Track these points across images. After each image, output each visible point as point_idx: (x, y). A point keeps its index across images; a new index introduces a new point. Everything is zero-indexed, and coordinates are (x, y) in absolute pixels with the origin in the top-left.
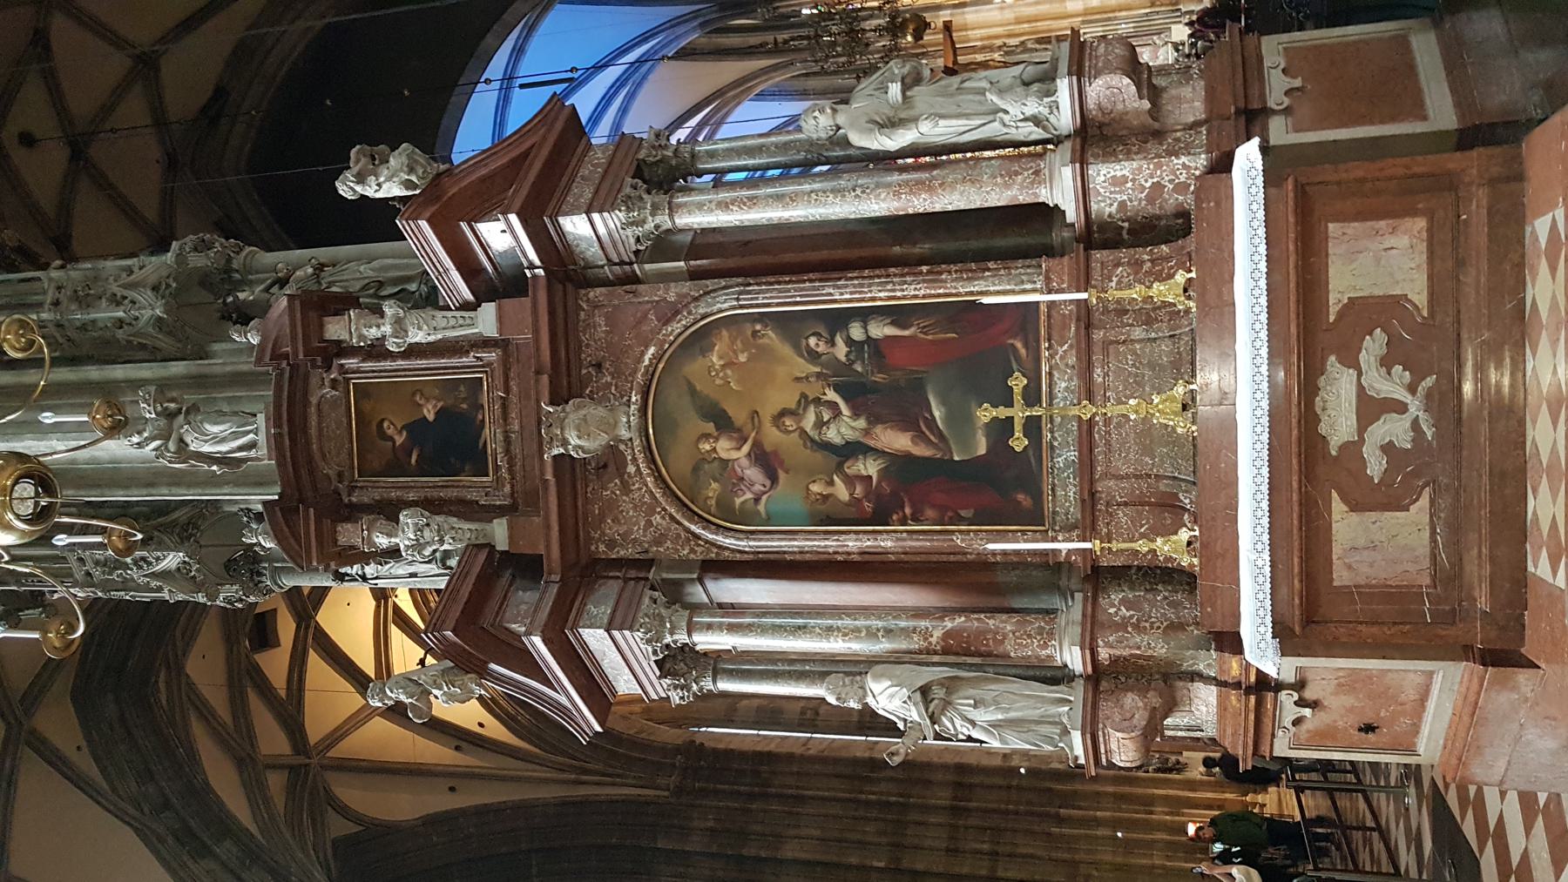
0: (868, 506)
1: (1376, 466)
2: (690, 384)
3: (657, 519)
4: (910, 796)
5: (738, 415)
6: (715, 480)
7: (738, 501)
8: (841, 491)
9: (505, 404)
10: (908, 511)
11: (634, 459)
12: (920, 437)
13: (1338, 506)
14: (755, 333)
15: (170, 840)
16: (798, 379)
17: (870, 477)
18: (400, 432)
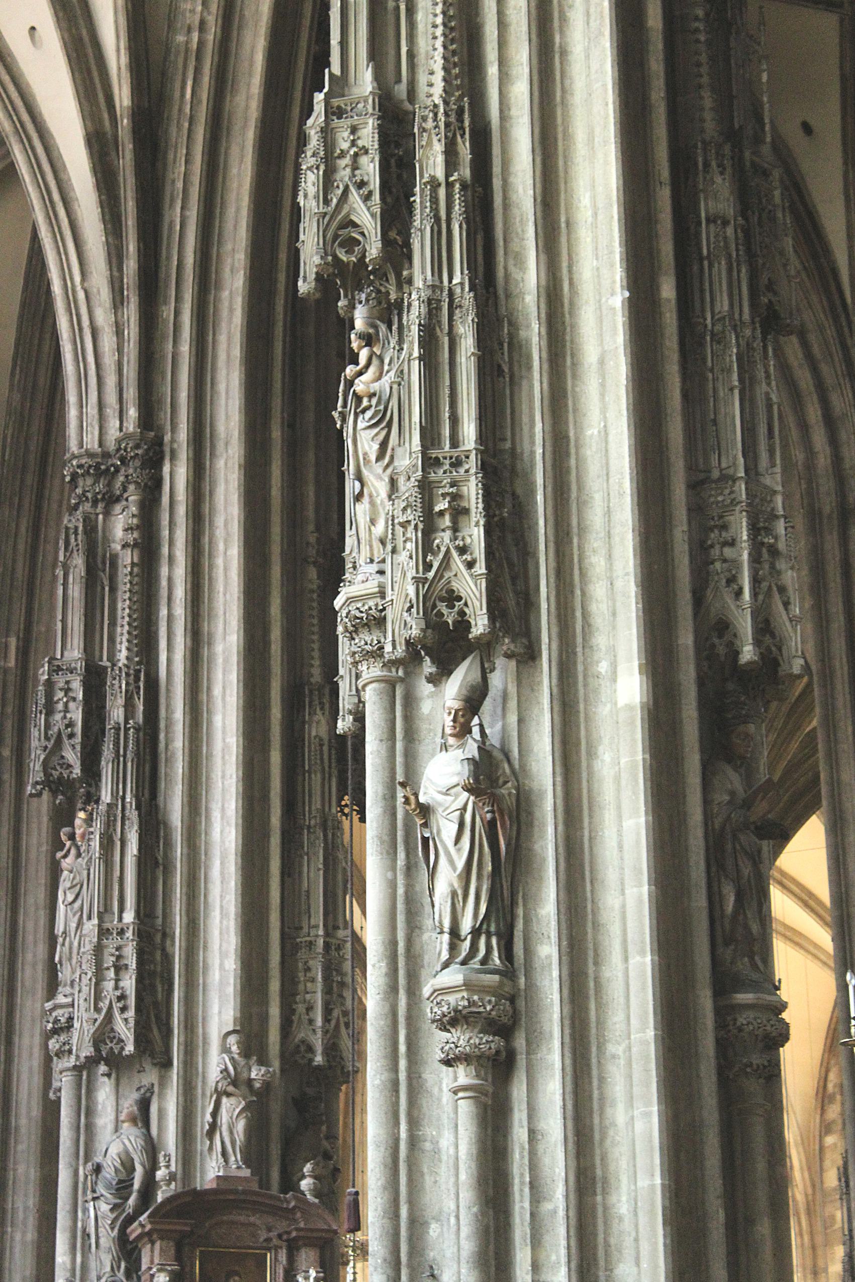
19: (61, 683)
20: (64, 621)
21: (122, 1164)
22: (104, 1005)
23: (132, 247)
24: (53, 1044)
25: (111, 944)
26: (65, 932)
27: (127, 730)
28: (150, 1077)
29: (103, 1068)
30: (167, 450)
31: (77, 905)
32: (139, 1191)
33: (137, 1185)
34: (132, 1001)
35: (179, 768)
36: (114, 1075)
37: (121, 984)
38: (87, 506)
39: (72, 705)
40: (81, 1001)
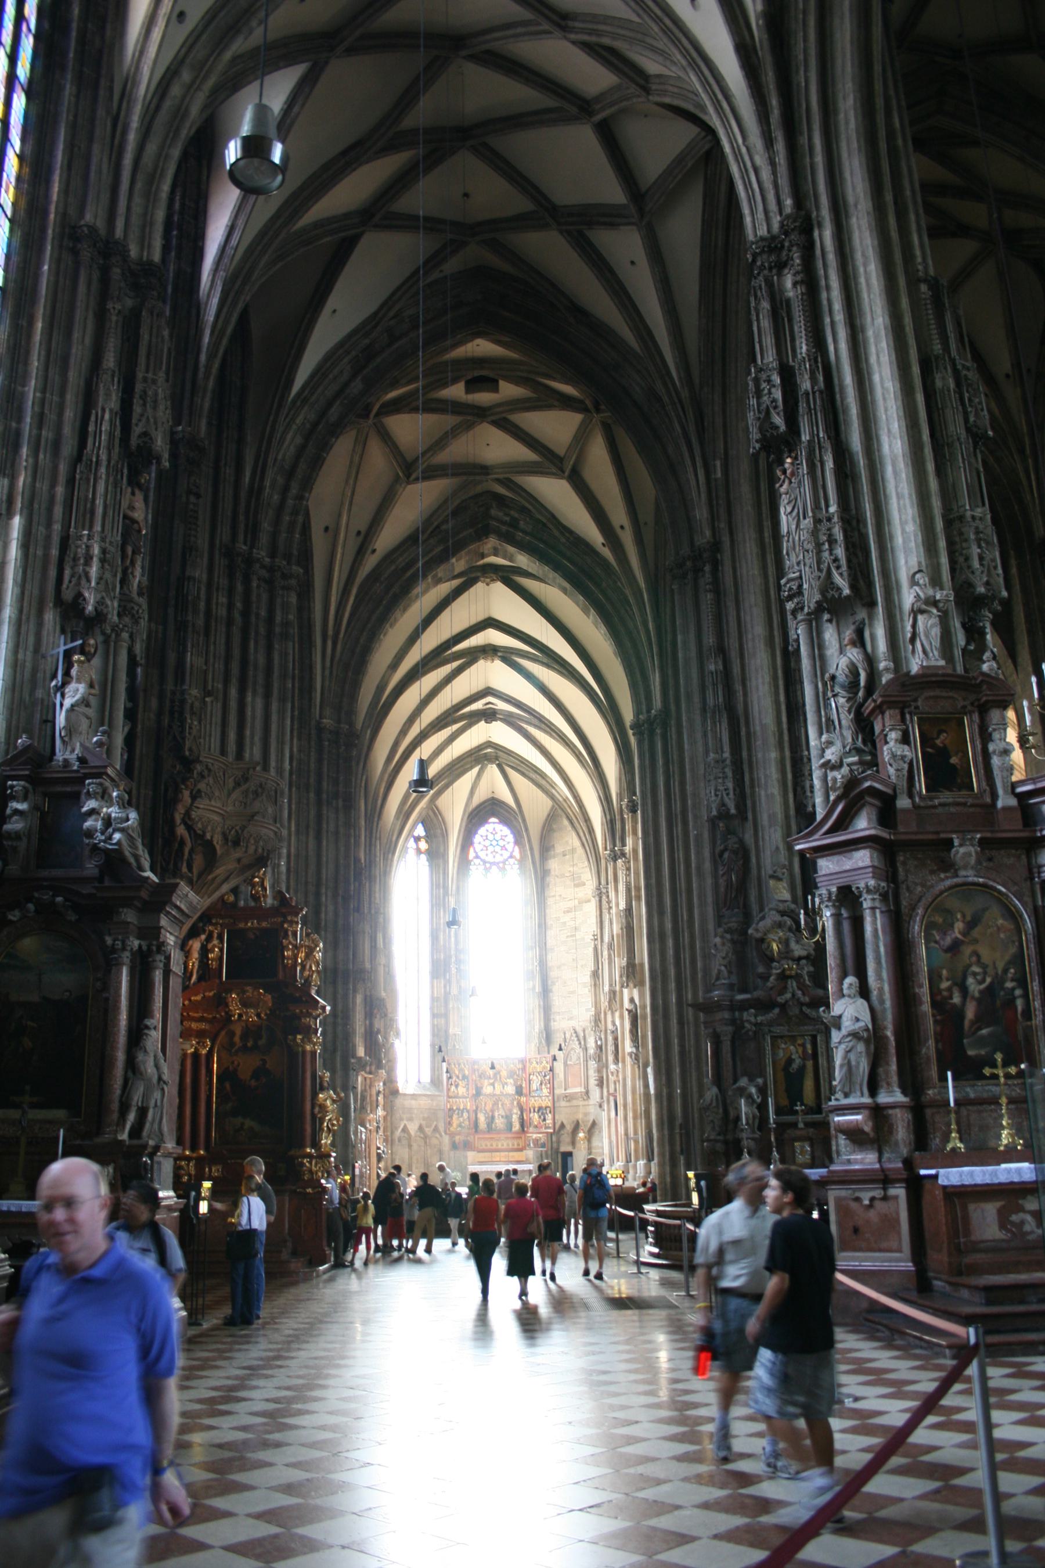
0: (939, 998)
1: (1014, 1218)
2: (987, 909)
3: (919, 889)
4: (326, 931)
5: (976, 933)
6: (944, 921)
7: (934, 932)
8: (945, 985)
9: (964, 804)
10: (938, 1018)
11: (947, 878)
12: (973, 1023)
13: (999, 1204)
14: (1013, 942)
15: (367, 341)
16: (994, 963)
17: (951, 998)
18: (942, 743)
19: (763, 376)
20: (760, 342)
21: (850, 671)
22: (824, 567)
23: (774, 102)
24: (790, 606)
25: (823, 528)
26: (788, 532)
27: (814, 393)
28: (862, 614)
29: (826, 616)
30: (815, 222)
31: (795, 513)
32: (865, 687)
33: (862, 683)
34: (843, 562)
35: (854, 411)
36: (834, 622)
37: (834, 552)
38: (766, 272)
39: (773, 390)
40: (807, 569)
